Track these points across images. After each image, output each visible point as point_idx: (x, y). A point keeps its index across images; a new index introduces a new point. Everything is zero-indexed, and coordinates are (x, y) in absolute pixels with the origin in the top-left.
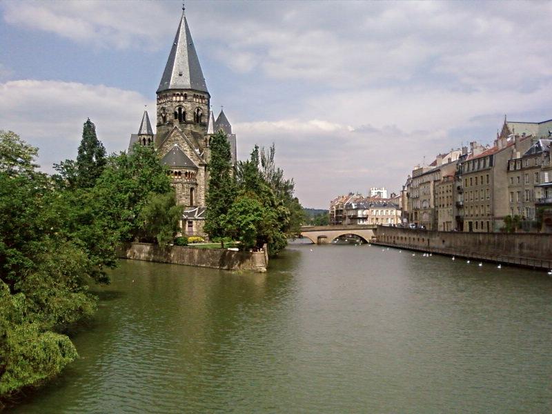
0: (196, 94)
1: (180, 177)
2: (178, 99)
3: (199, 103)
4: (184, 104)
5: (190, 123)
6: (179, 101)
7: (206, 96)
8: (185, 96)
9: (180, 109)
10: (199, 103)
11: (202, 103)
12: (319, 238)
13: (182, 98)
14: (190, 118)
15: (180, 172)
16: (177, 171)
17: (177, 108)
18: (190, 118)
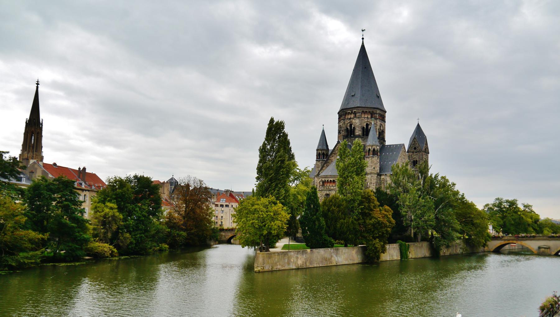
0: (365, 111)
1: (334, 185)
2: (349, 117)
3: (368, 118)
4: (354, 121)
5: (359, 136)
6: (350, 118)
7: (378, 112)
8: (355, 113)
9: (351, 125)
10: (368, 118)
11: (372, 117)
12: (539, 248)
13: (352, 116)
14: (358, 132)
15: (334, 181)
16: (332, 180)
17: (349, 124)
18: (358, 132)
